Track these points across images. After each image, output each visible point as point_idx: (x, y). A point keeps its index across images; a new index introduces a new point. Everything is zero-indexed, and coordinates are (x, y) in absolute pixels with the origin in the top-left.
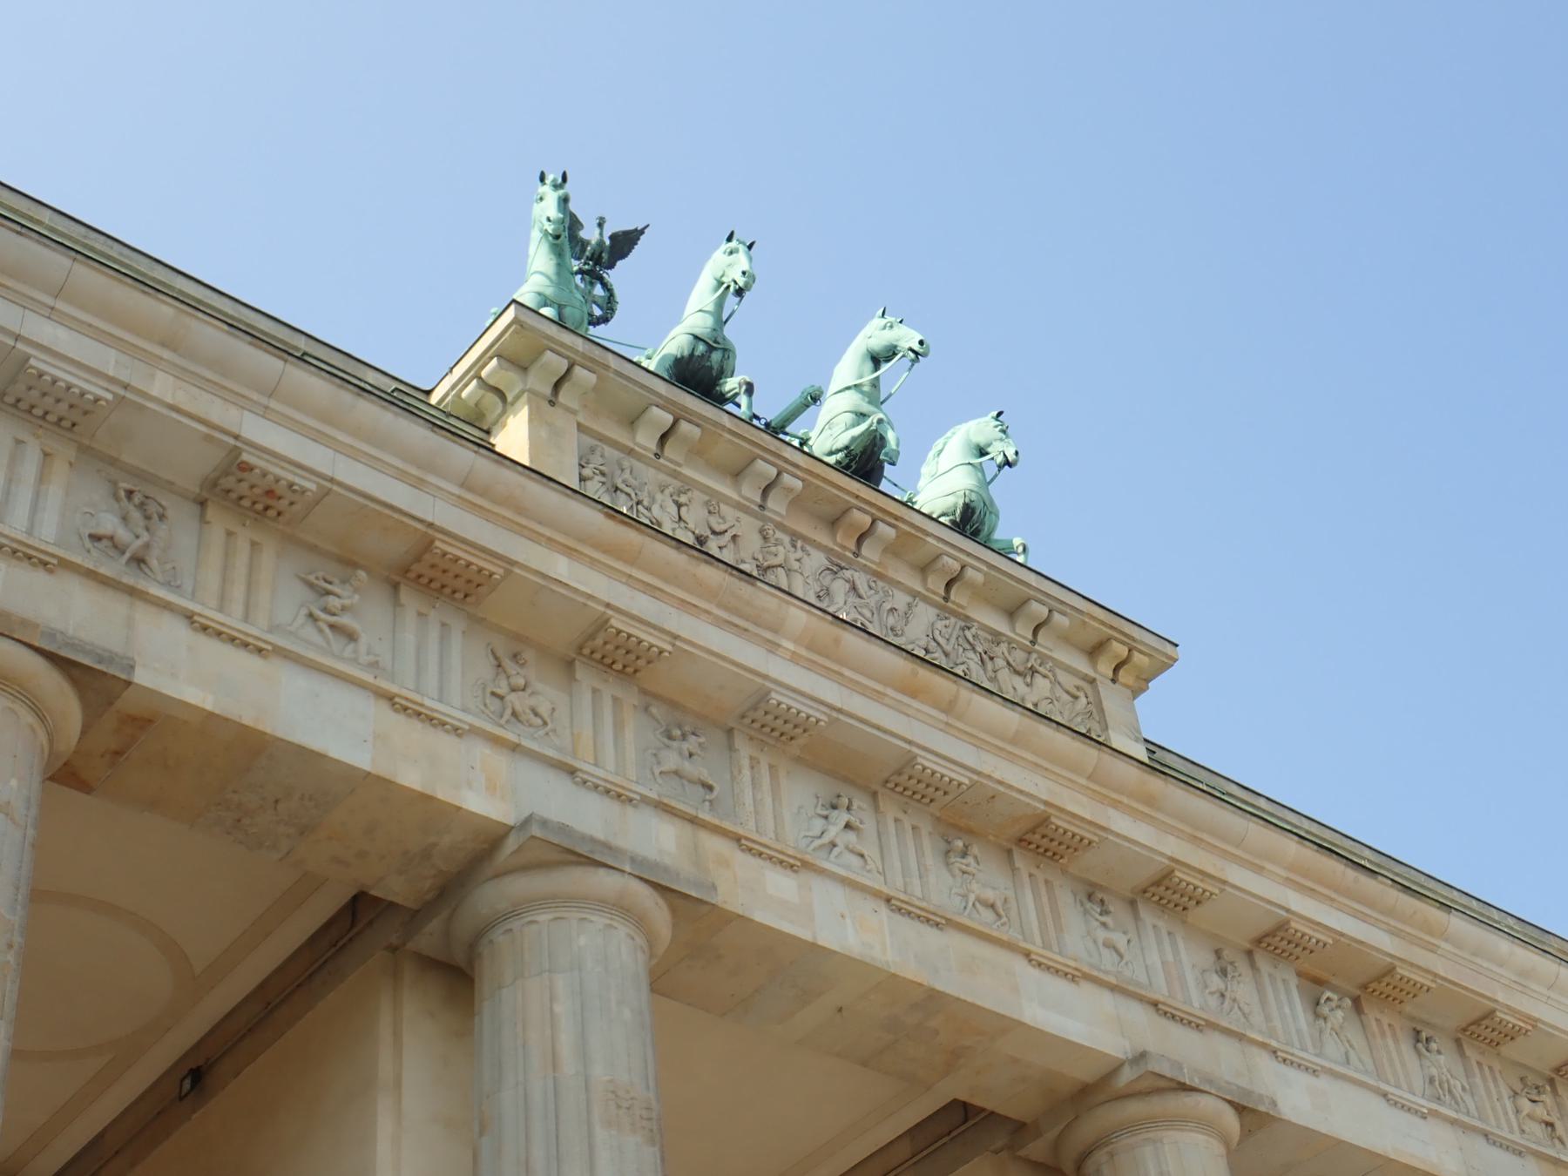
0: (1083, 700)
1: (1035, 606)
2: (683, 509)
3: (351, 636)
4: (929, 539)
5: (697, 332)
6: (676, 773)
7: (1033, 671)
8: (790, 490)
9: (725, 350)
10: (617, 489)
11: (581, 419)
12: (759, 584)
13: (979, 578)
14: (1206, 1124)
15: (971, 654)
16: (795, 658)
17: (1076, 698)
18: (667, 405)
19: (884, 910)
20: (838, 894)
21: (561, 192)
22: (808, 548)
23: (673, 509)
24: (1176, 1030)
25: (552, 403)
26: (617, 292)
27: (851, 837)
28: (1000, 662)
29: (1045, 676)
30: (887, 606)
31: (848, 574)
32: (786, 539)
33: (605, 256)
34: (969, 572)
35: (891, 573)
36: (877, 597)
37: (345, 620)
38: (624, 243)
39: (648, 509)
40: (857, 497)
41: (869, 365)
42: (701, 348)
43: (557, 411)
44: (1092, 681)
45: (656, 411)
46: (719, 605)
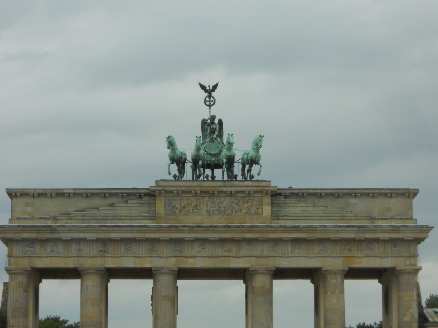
3: (130, 250)
6: (176, 250)
7: (248, 201)
9: (199, 156)
11: (165, 196)
14: (262, 273)
16: (188, 233)
18: (175, 190)
19: (208, 259)
20: (200, 259)
21: (169, 140)
23: (180, 205)
24: (261, 260)
25: (160, 195)
26: (215, 98)
27: (203, 250)
32: (201, 198)
37: (129, 249)
38: (215, 87)
42: (195, 157)
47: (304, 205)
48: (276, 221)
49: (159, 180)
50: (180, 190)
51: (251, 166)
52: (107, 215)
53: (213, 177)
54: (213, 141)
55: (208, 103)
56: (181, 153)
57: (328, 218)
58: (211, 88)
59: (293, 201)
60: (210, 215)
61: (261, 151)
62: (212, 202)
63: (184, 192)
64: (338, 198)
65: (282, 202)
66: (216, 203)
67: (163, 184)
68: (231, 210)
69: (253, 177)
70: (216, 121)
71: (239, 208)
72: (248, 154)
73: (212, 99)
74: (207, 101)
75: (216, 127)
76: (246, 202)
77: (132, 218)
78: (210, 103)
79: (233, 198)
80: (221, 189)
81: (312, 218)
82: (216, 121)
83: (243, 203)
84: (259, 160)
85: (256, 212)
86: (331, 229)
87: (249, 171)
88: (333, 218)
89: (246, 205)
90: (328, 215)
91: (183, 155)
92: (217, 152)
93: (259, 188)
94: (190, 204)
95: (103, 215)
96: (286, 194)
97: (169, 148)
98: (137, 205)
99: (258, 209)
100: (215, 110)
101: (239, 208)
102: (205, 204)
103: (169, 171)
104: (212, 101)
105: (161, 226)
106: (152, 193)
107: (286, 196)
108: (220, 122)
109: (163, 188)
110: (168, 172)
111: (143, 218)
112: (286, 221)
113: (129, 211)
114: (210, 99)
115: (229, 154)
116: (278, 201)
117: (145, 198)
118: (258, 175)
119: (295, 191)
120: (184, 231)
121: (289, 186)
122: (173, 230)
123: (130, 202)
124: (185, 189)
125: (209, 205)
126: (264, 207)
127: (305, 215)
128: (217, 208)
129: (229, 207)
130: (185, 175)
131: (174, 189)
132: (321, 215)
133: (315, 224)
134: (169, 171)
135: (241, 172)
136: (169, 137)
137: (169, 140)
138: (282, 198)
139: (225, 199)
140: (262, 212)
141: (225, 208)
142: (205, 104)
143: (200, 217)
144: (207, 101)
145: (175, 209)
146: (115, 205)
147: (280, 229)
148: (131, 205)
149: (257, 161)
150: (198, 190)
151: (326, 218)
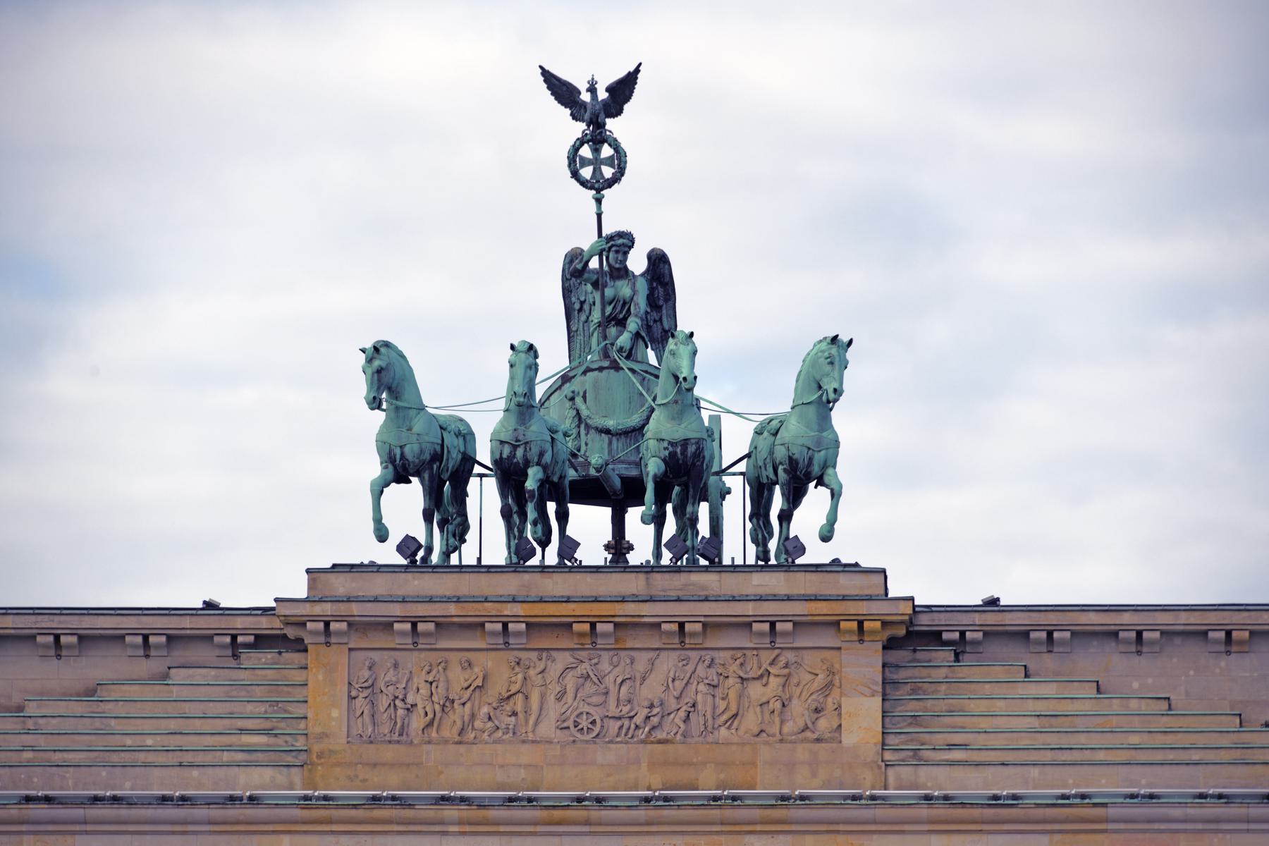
9: (526, 443)
18: (403, 619)
21: (377, 363)
22: (554, 654)
23: (424, 691)
25: (328, 644)
28: (731, 681)
30: (619, 680)
32: (534, 655)
33: (602, 115)
35: (629, 644)
36: (617, 669)
38: (623, 89)
41: (672, 380)
42: (507, 451)
43: (333, 647)
44: (839, 648)
45: (396, 626)
46: (398, 823)
47: (1050, 690)
48: (906, 772)
49: (329, 566)
50: (425, 619)
51: (795, 496)
52: (62, 742)
53: (619, 546)
54: (616, 367)
55: (587, 173)
57: (1171, 756)
58: (603, 95)
59: (998, 673)
61: (840, 418)
62: (589, 676)
63: (443, 626)
64: (1228, 653)
65: (939, 674)
66: (608, 681)
67: (342, 586)
68: (682, 714)
69: (801, 550)
70: (637, 263)
72: (776, 434)
73: (607, 151)
74: (585, 162)
75: (635, 292)
77: (188, 758)
78: (597, 171)
79: (694, 655)
80: (631, 609)
81: (1088, 755)
82: (637, 263)
84: (830, 463)
85: (806, 728)
86: (1177, 812)
87: (785, 517)
88: (1196, 756)
89: (756, 691)
90: (1169, 740)
91: (449, 440)
92: (635, 420)
95: (41, 742)
96: (963, 634)
98: (217, 693)
99: (817, 710)
100: (621, 210)
104: (609, 161)
105: (326, 798)
106: (291, 633)
107: (960, 647)
108: (658, 261)
109: (343, 609)
110: (370, 526)
112: (958, 772)
113: (173, 725)
114: (596, 151)
115: (678, 432)
116: (916, 672)
117: (251, 658)
118: (826, 537)
119: (1008, 619)
120: (441, 822)
121: (987, 595)
122: (389, 822)
123: (178, 675)
124: (452, 609)
125: (570, 695)
127: (1053, 740)
128: (613, 710)
129: (673, 704)
130: (472, 536)
131: (397, 610)
132: (1135, 739)
133: (1105, 784)
135: (749, 525)
136: (376, 349)
137: (377, 363)
138: (946, 655)
139: (652, 663)
140: (840, 725)
141: (651, 706)
142: (575, 175)
143: (527, 754)
144: (585, 162)
145: (400, 712)
146: (102, 693)
147: (924, 812)
148: (186, 693)
149: (816, 469)
150: (517, 618)
151: (1159, 756)
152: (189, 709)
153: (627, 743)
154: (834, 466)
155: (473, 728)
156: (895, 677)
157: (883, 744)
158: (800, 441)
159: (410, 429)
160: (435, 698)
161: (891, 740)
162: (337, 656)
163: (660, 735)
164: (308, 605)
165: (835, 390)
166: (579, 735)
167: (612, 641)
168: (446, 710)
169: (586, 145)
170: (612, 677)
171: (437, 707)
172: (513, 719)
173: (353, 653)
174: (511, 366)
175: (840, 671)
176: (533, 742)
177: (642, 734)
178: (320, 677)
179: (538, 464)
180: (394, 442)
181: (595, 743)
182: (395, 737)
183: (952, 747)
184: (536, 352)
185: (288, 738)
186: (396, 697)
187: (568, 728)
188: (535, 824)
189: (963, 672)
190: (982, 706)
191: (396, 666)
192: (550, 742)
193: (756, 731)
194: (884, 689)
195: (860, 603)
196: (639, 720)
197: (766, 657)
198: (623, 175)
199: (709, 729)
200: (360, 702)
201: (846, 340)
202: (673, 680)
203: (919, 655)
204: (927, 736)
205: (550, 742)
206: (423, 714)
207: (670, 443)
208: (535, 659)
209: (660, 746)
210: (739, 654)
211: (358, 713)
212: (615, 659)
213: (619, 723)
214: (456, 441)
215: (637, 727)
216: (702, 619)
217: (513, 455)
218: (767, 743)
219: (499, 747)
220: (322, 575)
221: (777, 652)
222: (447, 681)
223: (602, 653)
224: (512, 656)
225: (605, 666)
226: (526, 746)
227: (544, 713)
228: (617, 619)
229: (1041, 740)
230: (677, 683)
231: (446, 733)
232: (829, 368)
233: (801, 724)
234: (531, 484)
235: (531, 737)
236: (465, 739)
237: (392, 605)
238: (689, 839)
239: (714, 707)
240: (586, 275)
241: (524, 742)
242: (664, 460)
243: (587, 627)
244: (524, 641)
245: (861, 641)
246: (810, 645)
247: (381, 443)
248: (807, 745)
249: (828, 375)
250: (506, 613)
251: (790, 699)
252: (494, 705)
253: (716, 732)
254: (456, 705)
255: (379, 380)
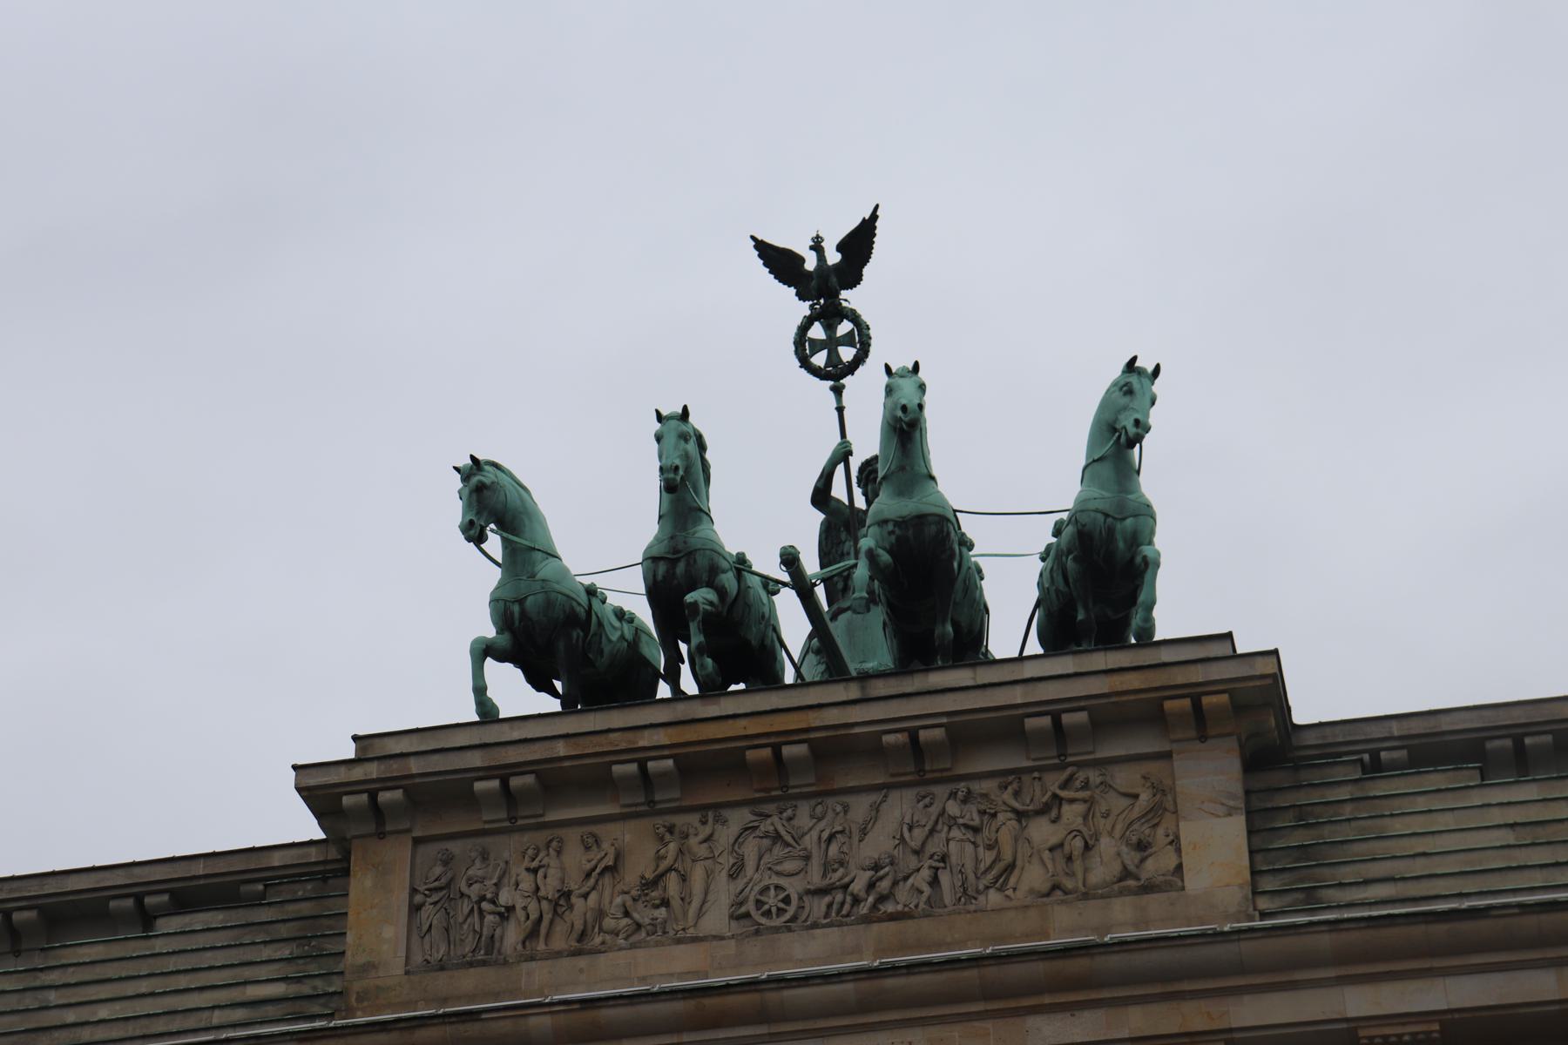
0: (1145, 797)
1: (1031, 723)
2: (541, 873)
4: (857, 730)
5: (655, 553)
8: (664, 774)
9: (691, 554)
10: (462, 895)
11: (417, 833)
12: (484, 1016)
13: (939, 733)
15: (955, 833)
17: (1136, 796)
18: (487, 773)
21: (475, 480)
22: (726, 813)
23: (527, 883)
25: (381, 835)
26: (866, 317)
28: (1001, 817)
29: (1072, 801)
30: (825, 835)
31: (766, 826)
32: (694, 819)
34: (923, 734)
35: (840, 783)
36: (822, 825)
38: (859, 244)
39: (493, 902)
40: (746, 737)
42: (662, 568)
44: (1167, 756)
45: (479, 786)
47: (1529, 792)
55: (820, 359)
56: (591, 591)
58: (833, 257)
60: (757, 933)
62: (777, 837)
65: (1343, 793)
66: (809, 841)
68: (926, 873)
71: (988, 857)
73: (845, 327)
74: (817, 346)
76: (1043, 811)
78: (833, 358)
79: (941, 791)
80: (833, 717)
83: (1020, 815)
85: (1126, 874)
89: (1042, 832)
93: (1133, 681)
94: (612, 869)
96: (1375, 755)
97: (478, 538)
101: (988, 857)
102: (727, 861)
103: (480, 690)
104: (848, 340)
107: (1375, 768)
109: (395, 768)
111: (239, 1014)
113: (144, 986)
114: (830, 328)
116: (1302, 798)
119: (1446, 724)
124: (561, 749)
126: (1189, 831)
128: (816, 878)
129: (913, 862)
131: (475, 760)
134: (480, 690)
137: (475, 480)
139: (876, 808)
140: (1180, 867)
141: (876, 867)
142: (805, 363)
144: (817, 346)
149: (1121, 545)
152: (172, 964)
153: (841, 925)
154: (1151, 543)
155: (601, 929)
156: (1269, 805)
157: (1254, 884)
158: (1092, 505)
159: (533, 576)
160: (542, 893)
161: (1268, 884)
162: (397, 853)
163: (889, 907)
164: (343, 769)
165: (1137, 423)
166: (763, 920)
167: (812, 780)
168: (560, 910)
169: (817, 325)
170: (814, 834)
171: (545, 904)
172: (663, 910)
173: (422, 849)
174: (659, 438)
175: (1173, 789)
176: (695, 940)
177: (864, 909)
178: (368, 883)
179: (710, 584)
180: (508, 594)
181: (789, 930)
182: (480, 956)
183: (1367, 882)
184: (700, 439)
185: (319, 983)
186: (483, 898)
187: (747, 915)
188: (679, 1030)
189: (1380, 788)
190: (1417, 824)
191: (485, 856)
192: (722, 938)
193: (1045, 887)
194: (1247, 802)
195: (1192, 668)
196: (858, 887)
197: (1053, 781)
198: (867, 356)
199: (970, 892)
200: (424, 913)
201: (1150, 369)
202: (910, 829)
203: (1307, 776)
204: (1326, 871)
205: (722, 938)
206: (520, 914)
207: (897, 523)
208: (697, 824)
209: (892, 926)
210: (1011, 778)
211: (425, 928)
212: (819, 809)
213: (827, 899)
214: (617, 624)
215: (856, 901)
216: (944, 720)
217: (670, 574)
218: (1063, 902)
219: (640, 953)
220: (377, 741)
221: (1070, 770)
222: (563, 869)
223: (799, 803)
224: (659, 821)
225: (803, 819)
226: (682, 947)
227: (711, 897)
228: (812, 735)
229: (1522, 857)
230: (916, 831)
231: (559, 943)
232: (1126, 400)
233: (1116, 868)
234: (689, 598)
235: (691, 932)
236: (587, 946)
237: (469, 754)
238: (936, 1032)
239: (977, 861)
240: (833, 503)
241: (679, 941)
242: (889, 552)
243: (766, 753)
244: (677, 794)
245: (1203, 738)
246: (1119, 751)
247: (495, 601)
248: (1128, 899)
249: (1125, 408)
250: (642, 743)
251: (1096, 836)
252: (634, 893)
253: (982, 898)
254: (574, 899)
255: (479, 502)
